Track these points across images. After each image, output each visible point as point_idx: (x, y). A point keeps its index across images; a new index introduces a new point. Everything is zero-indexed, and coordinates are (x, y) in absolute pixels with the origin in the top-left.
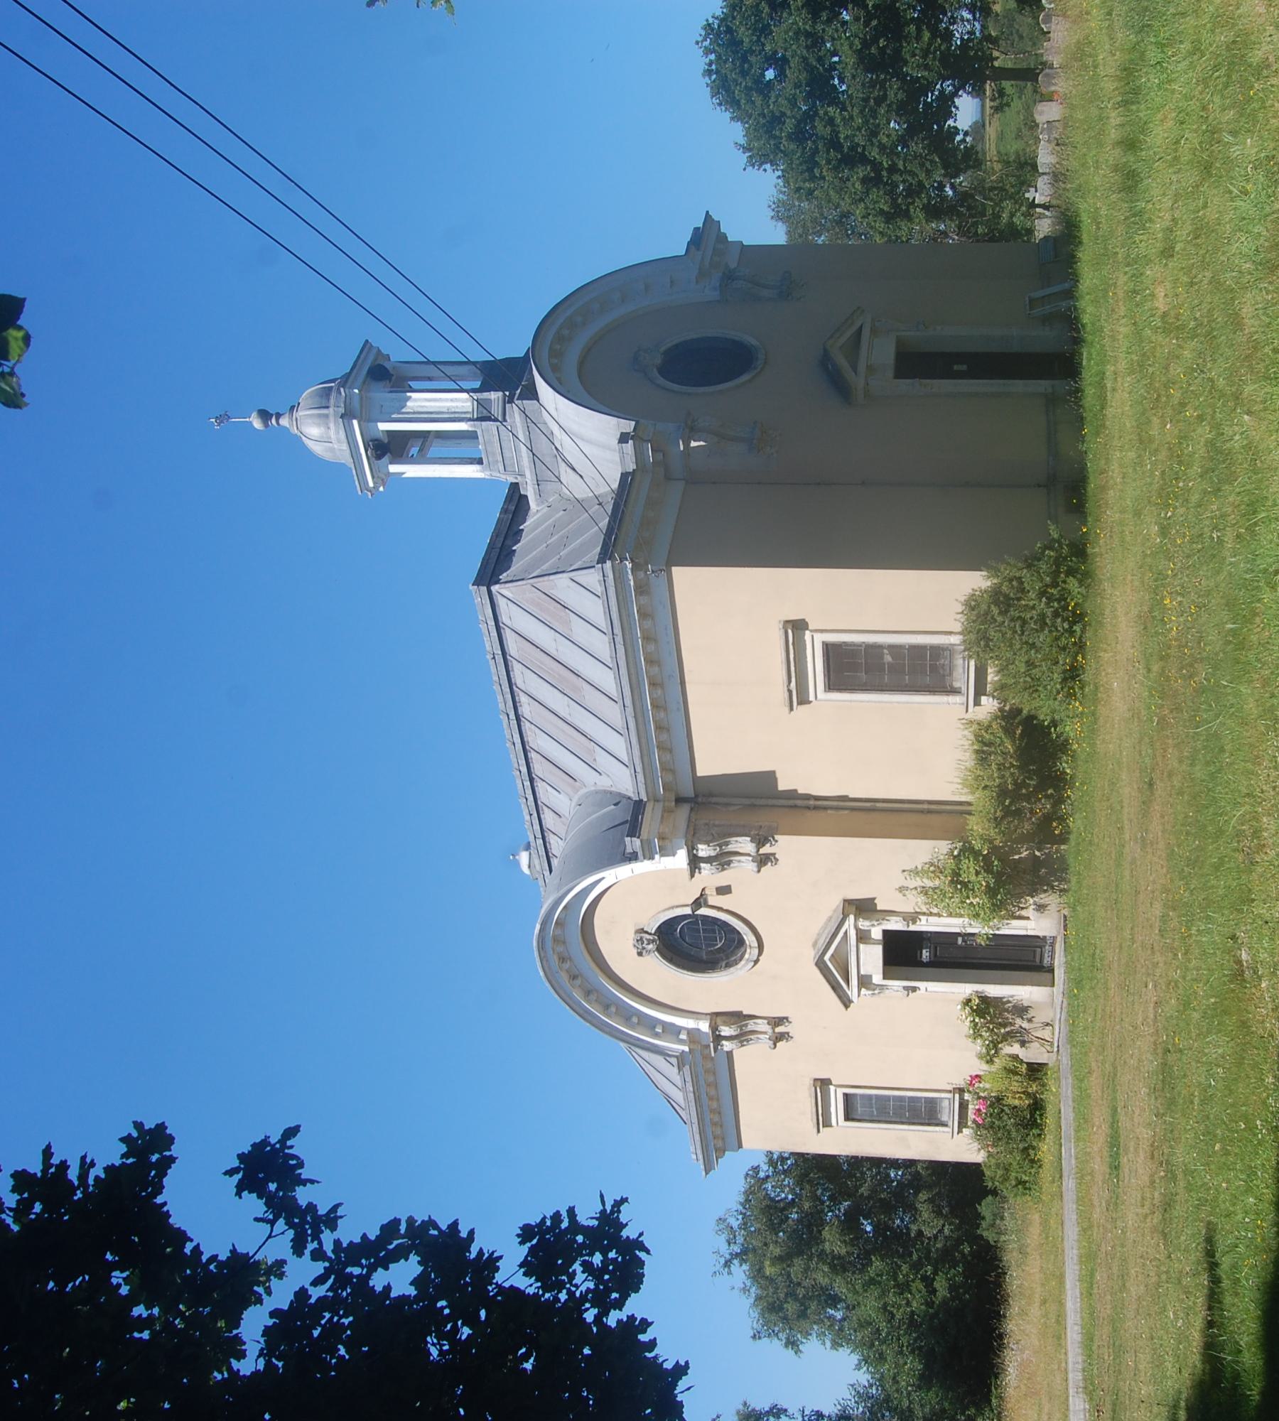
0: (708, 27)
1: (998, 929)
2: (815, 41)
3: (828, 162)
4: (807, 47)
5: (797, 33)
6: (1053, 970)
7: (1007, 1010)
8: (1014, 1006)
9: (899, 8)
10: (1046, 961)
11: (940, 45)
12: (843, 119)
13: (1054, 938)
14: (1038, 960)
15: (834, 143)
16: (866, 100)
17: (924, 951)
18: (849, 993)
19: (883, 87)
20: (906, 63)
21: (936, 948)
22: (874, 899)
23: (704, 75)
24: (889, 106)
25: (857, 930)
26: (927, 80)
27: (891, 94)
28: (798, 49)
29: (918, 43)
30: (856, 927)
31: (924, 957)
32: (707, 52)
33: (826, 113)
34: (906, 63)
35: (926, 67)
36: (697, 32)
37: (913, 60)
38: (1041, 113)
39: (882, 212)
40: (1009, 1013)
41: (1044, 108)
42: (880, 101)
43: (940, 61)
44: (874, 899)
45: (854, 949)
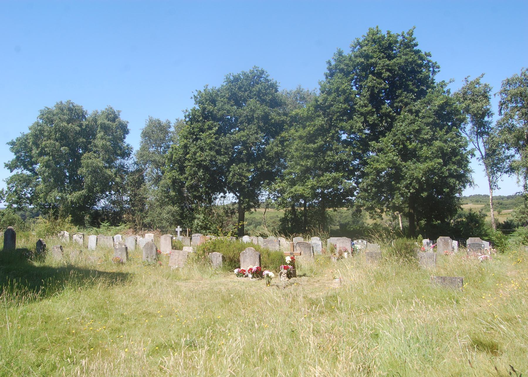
0: (262, 72)
2: (250, 120)
3: (193, 128)
4: (247, 116)
5: (254, 111)
9: (262, 160)
11: (244, 182)
12: (210, 134)
15: (202, 130)
16: (220, 146)
19: (225, 153)
20: (237, 165)
23: (243, 72)
24: (215, 157)
26: (228, 176)
27: (222, 158)
28: (245, 111)
29: (246, 170)
32: (252, 72)
33: (215, 126)
34: (237, 165)
35: (234, 175)
36: (262, 66)
37: (237, 168)
38: (165, 239)
39: (172, 155)
41: (168, 241)
42: (218, 152)
43: (236, 181)
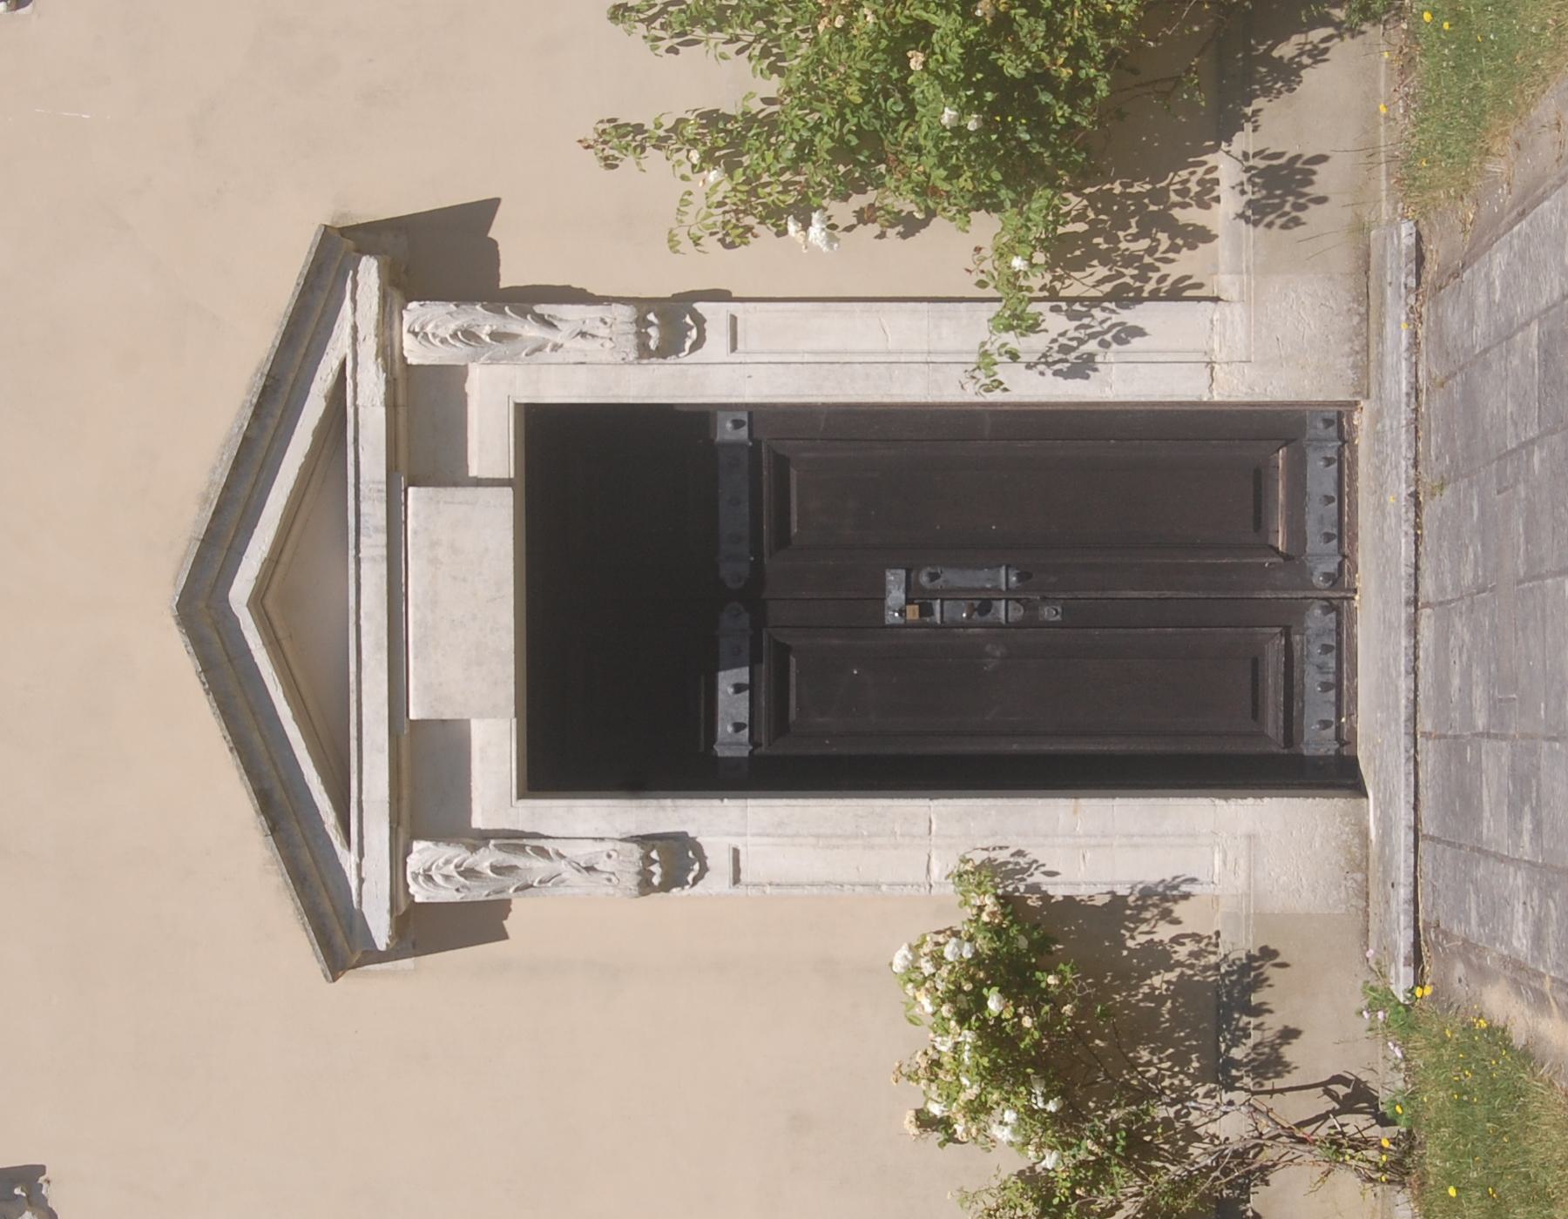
1: (1083, 368)
6: (1354, 761)
7: (1143, 1027)
8: (1182, 987)
10: (1317, 742)
13: (1338, 420)
14: (1273, 724)
17: (728, 680)
18: (348, 860)
21: (783, 652)
22: (486, 210)
25: (388, 368)
30: (388, 353)
31: (725, 729)
40: (1161, 1041)
44: (486, 210)
45: (374, 512)
